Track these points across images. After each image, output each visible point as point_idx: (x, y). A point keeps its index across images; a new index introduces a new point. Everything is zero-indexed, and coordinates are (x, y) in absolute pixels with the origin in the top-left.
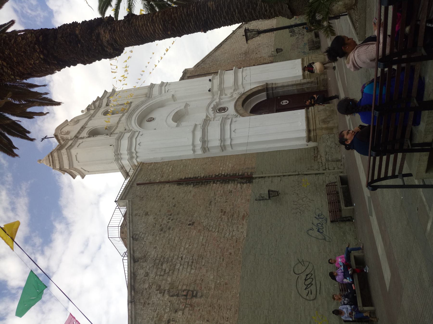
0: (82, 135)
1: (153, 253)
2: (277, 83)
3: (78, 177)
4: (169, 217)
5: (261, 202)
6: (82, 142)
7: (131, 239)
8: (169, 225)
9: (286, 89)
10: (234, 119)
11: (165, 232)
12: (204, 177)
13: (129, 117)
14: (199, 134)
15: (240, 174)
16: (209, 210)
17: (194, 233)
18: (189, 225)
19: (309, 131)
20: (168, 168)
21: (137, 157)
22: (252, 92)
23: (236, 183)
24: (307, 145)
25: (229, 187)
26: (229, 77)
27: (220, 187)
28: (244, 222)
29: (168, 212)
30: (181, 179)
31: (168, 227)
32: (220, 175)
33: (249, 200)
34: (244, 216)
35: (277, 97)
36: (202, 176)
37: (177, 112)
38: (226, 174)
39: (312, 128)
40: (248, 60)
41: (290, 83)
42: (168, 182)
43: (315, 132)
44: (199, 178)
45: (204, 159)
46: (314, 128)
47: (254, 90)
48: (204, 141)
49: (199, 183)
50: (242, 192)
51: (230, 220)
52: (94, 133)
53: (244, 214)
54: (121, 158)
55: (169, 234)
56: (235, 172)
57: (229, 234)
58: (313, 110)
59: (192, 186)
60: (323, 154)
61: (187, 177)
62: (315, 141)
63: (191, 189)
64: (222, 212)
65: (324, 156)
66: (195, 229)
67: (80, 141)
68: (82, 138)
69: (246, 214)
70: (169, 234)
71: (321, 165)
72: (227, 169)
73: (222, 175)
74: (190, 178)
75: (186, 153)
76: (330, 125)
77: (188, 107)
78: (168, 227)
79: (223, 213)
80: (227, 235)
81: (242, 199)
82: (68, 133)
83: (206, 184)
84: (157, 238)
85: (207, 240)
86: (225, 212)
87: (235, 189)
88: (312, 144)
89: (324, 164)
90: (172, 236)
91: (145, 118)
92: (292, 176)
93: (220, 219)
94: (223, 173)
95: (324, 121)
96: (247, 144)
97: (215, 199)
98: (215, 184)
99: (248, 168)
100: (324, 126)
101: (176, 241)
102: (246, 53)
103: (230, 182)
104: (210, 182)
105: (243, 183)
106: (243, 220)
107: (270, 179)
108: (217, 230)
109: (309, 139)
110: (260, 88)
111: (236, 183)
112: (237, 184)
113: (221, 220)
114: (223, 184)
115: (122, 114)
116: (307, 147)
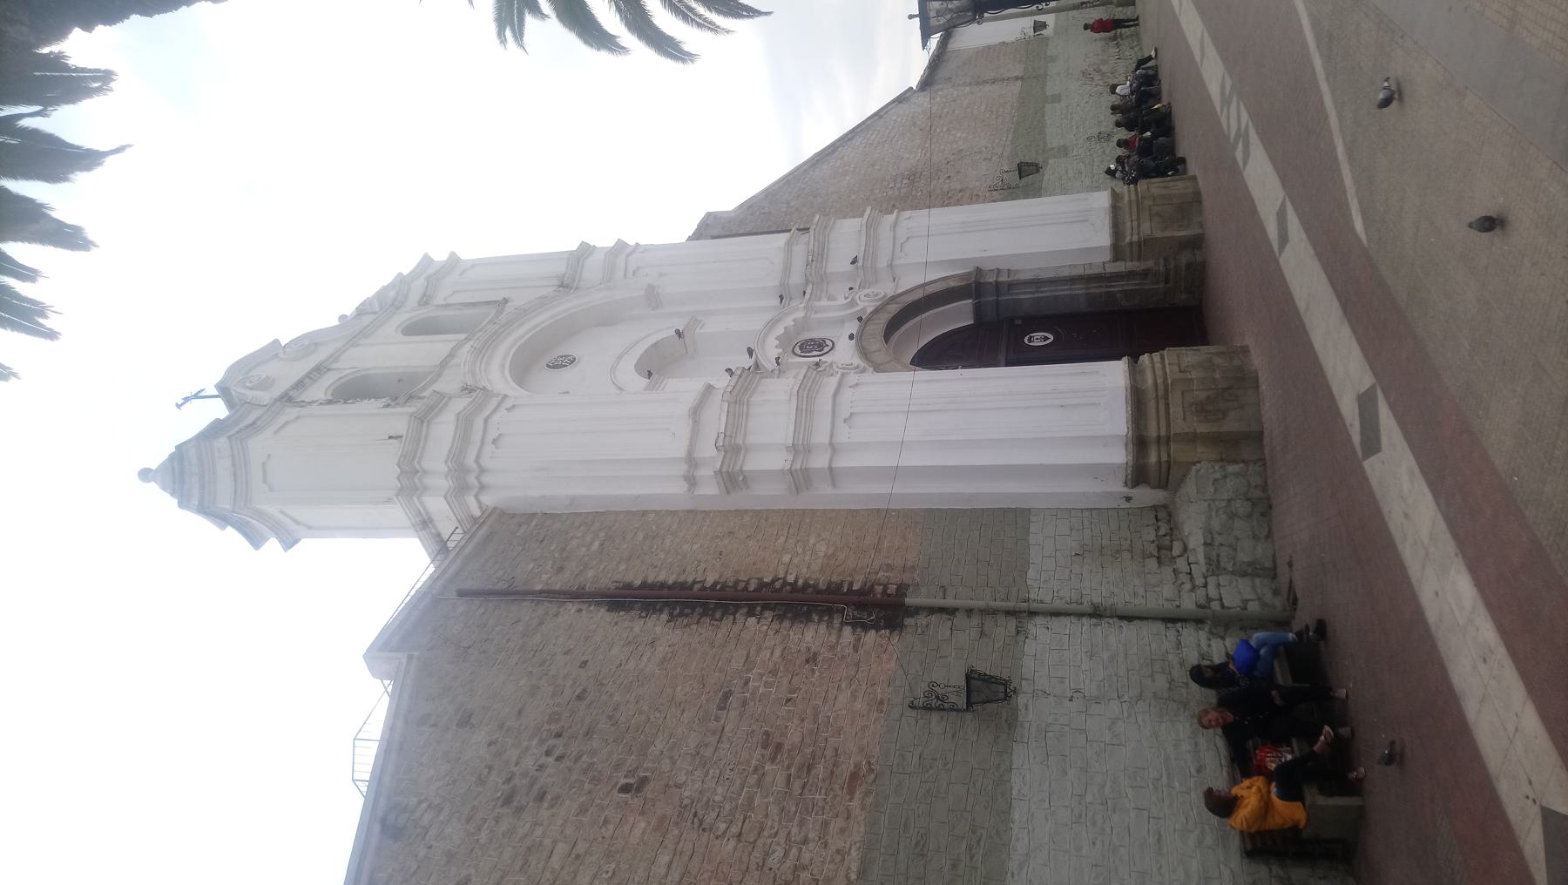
0: (308, 395)
2: (1017, 272)
3: (273, 544)
4: (552, 742)
5: (935, 717)
6: (298, 418)
9: (1047, 292)
10: (853, 378)
11: (519, 810)
12: (716, 583)
13: (484, 351)
14: (715, 419)
15: (855, 587)
16: (714, 733)
17: (637, 832)
18: (626, 789)
19: (1139, 443)
20: (588, 539)
21: (482, 487)
22: (918, 295)
23: (837, 621)
24: (1128, 499)
26: (847, 236)
27: (771, 633)
28: (855, 803)
29: (549, 722)
30: (628, 586)
31: (536, 787)
32: (778, 585)
33: (881, 702)
34: (854, 776)
36: (710, 581)
37: (655, 345)
38: (800, 582)
39: (1152, 432)
40: (921, 188)
41: (1066, 273)
42: (576, 595)
43: (1163, 448)
44: (697, 587)
45: (725, 514)
46: (1163, 433)
47: (931, 290)
48: (732, 448)
49: (693, 607)
50: (857, 665)
51: (797, 786)
52: (354, 391)
53: (857, 766)
54: (425, 488)
55: (536, 824)
56: (835, 578)
57: (786, 855)
58: (1158, 366)
59: (665, 617)
60: (1196, 541)
61: (650, 579)
62: (1163, 484)
63: (658, 629)
64: (765, 746)
65: (1201, 550)
66: (642, 813)
67: (292, 412)
68: (302, 404)
69: (864, 768)
70: (536, 824)
71: (1188, 586)
72: (804, 562)
73: (785, 583)
74: (663, 585)
75: (662, 487)
76: (1230, 425)
78: (536, 787)
79: (768, 752)
80: (773, 861)
81: (854, 697)
82: (265, 384)
83: (718, 615)
84: (483, 837)
85: (686, 872)
86: (779, 746)
87: (832, 648)
88: (1147, 496)
89: (1199, 581)
90: (544, 836)
91: (545, 356)
92: (1065, 620)
93: (753, 780)
94: (791, 579)
95: (1203, 409)
96: (896, 473)
97: (746, 683)
98: (752, 620)
99: (889, 567)
100: (1202, 428)
101: (555, 862)
102: (913, 177)
104: (737, 608)
105: (866, 628)
106: (851, 793)
107: (975, 620)
108: (734, 830)
109: (1139, 475)
110: (952, 284)
111: (837, 621)
112: (840, 630)
113: (759, 784)
114: (786, 623)
115: (462, 336)
116: (1127, 505)
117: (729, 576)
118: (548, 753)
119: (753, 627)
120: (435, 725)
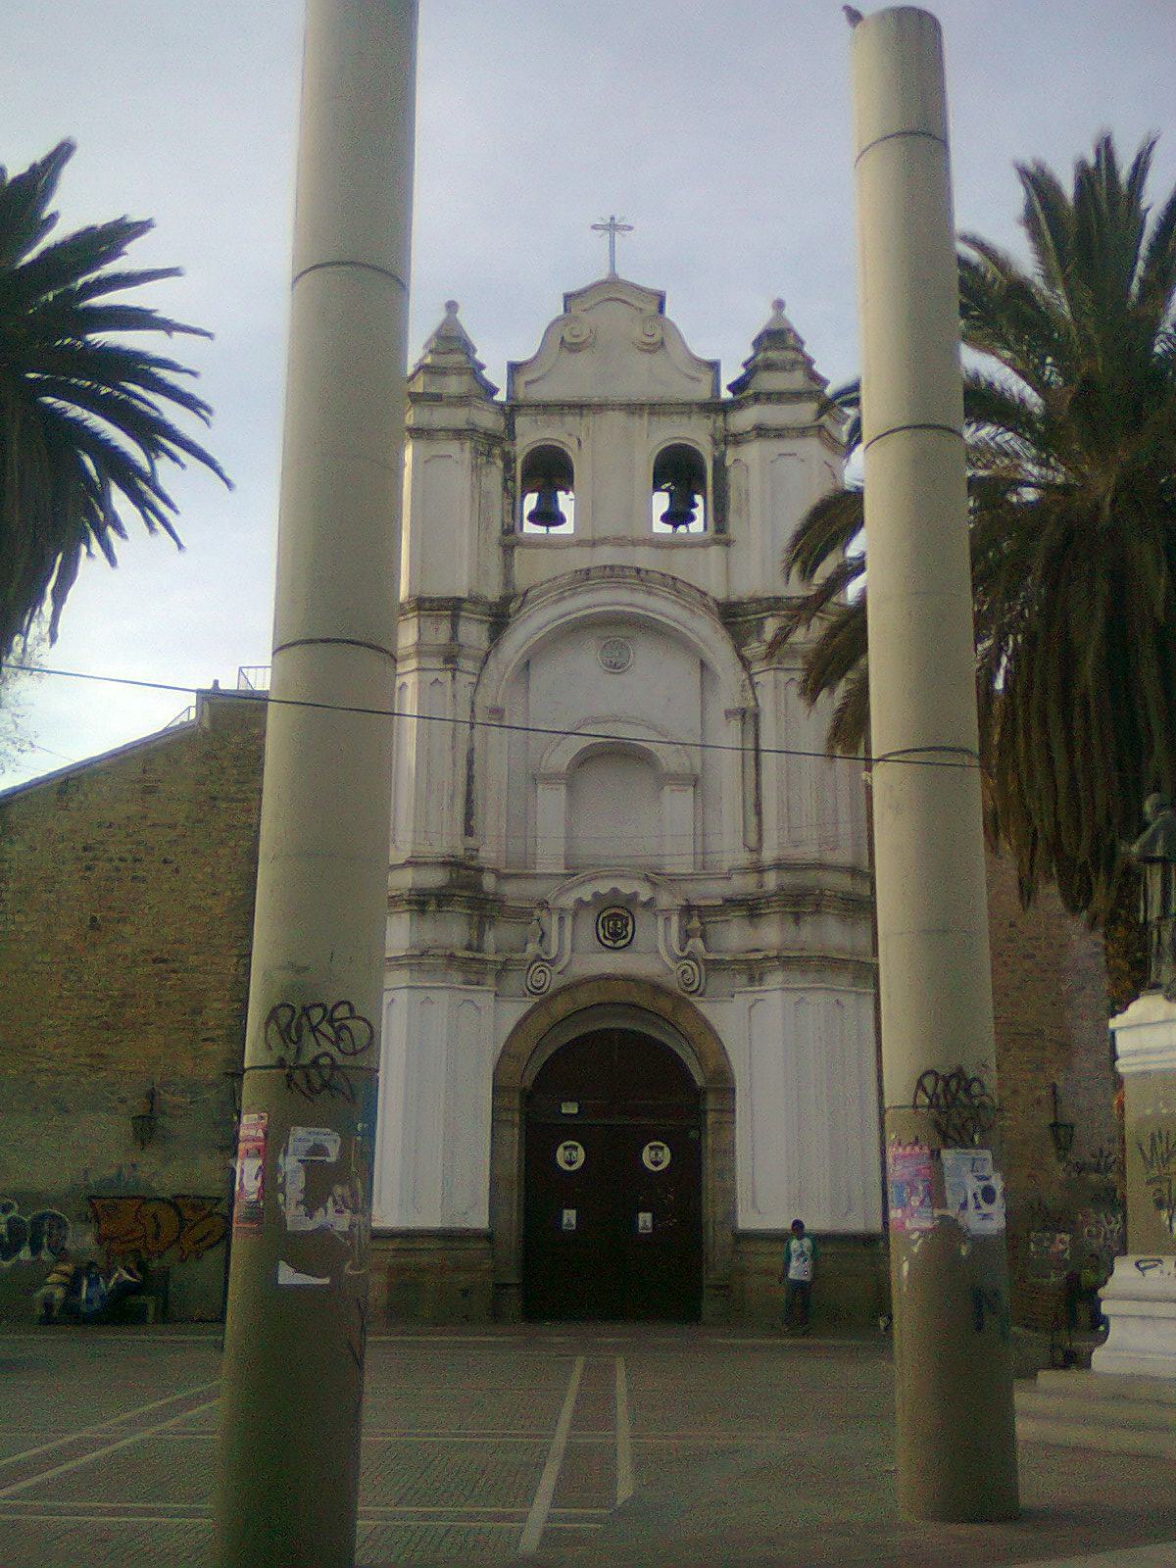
4: (130, 857)
7: (62, 779)
8: (101, 864)
18: (94, 919)
34: (101, 1056)
35: (700, 1127)
64: (124, 996)
66: (78, 935)
77: (667, 789)
86: (122, 1005)
101: (45, 896)
106: (90, 1055)
110: (711, 1064)
118: (121, 860)
120: (144, 771)
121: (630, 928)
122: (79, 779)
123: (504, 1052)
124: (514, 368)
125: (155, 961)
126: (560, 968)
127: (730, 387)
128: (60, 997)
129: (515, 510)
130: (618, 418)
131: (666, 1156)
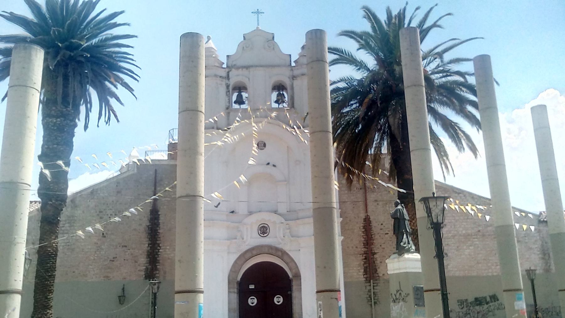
1: (78, 212)
15: (158, 267)
18: (103, 234)
25: (143, 259)
32: (159, 248)
34: (107, 277)
36: (160, 231)
56: (161, 261)
59: (148, 224)
80: (91, 267)
84: (92, 211)
86: (113, 261)
98: (147, 245)
99: (165, 273)
103: (149, 259)
114: (146, 253)
117: (161, 236)
118: (111, 215)
119: (145, 246)
121: (268, 231)
122: (97, 189)
123: (231, 270)
124: (228, 56)
125: (123, 246)
126: (247, 243)
127: (295, 62)
128: (94, 259)
129: (230, 101)
130: (260, 72)
131: (281, 300)
